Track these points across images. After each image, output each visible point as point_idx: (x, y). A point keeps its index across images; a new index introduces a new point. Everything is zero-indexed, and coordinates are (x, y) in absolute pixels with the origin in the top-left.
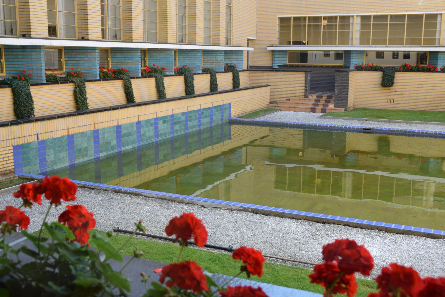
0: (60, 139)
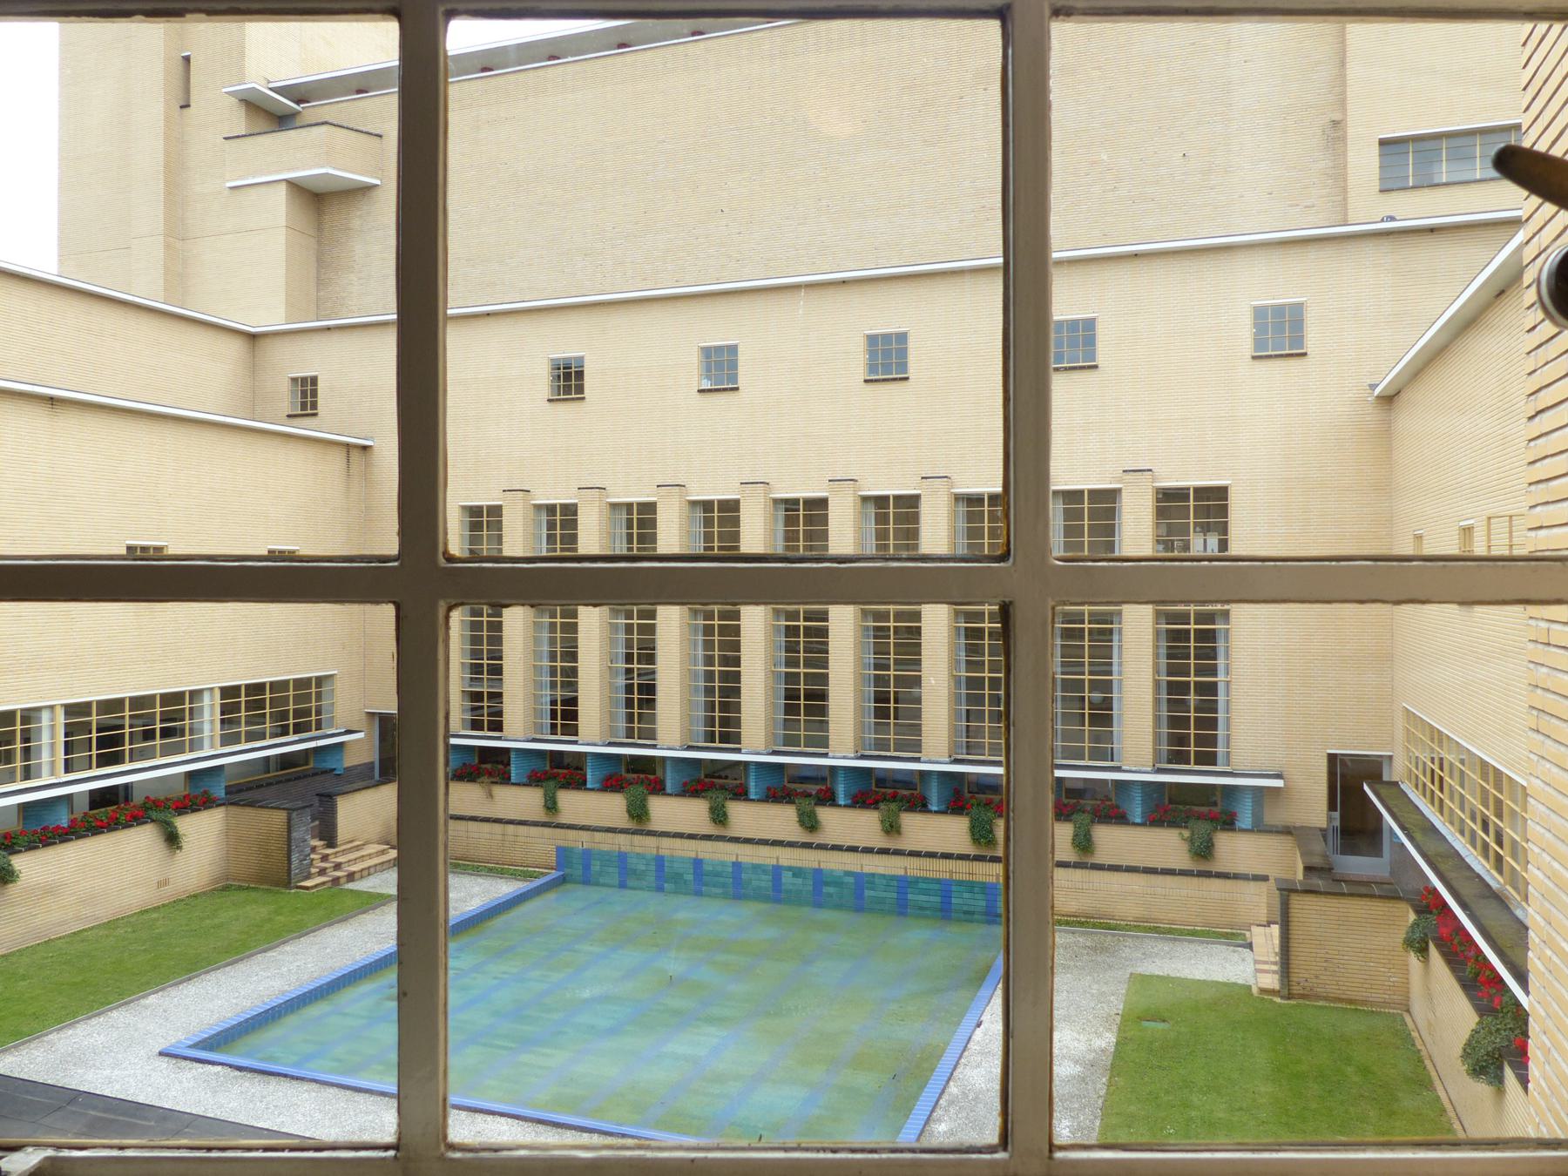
0: (608, 853)
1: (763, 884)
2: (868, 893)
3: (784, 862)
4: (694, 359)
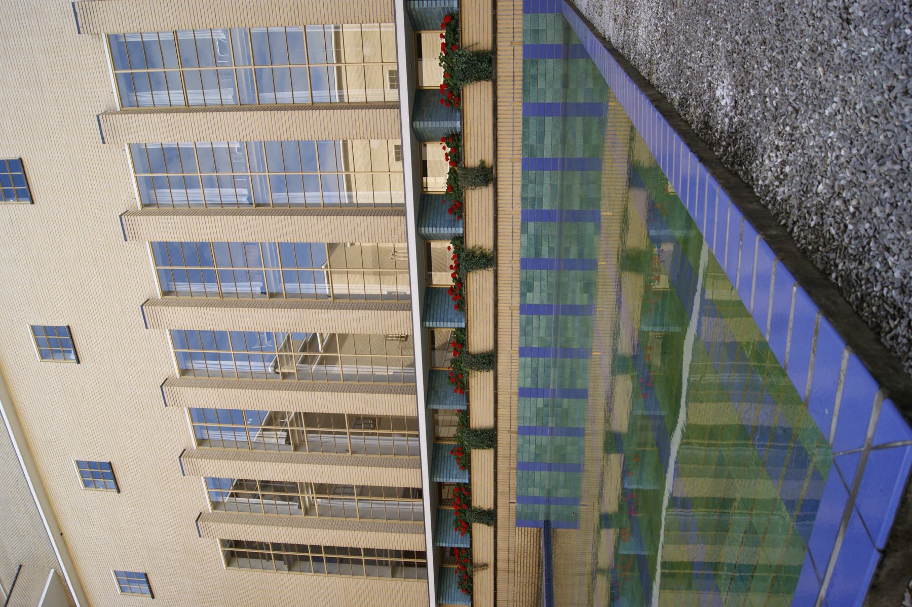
0: (519, 479)
1: (543, 325)
2: (546, 206)
3: (517, 300)
4: (51, 366)
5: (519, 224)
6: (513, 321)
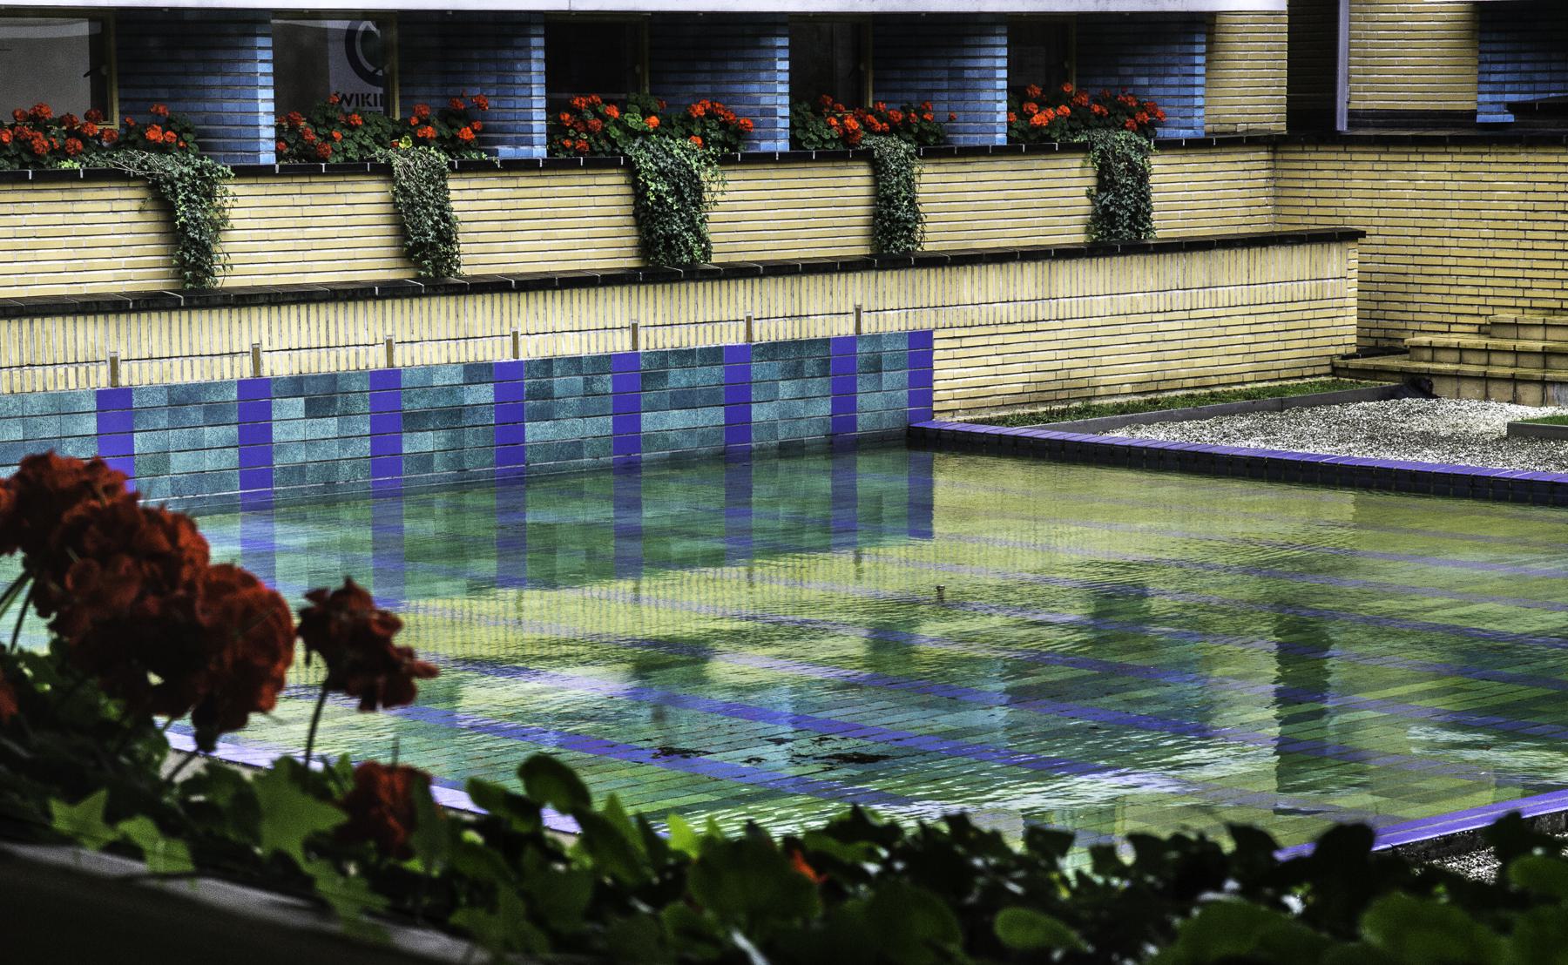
1: (209, 462)
2: (535, 432)
3: (277, 366)
5: (489, 358)
6: (217, 359)
